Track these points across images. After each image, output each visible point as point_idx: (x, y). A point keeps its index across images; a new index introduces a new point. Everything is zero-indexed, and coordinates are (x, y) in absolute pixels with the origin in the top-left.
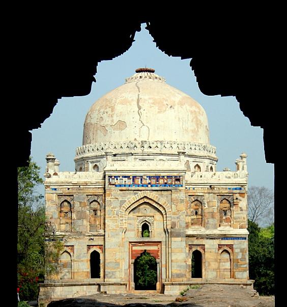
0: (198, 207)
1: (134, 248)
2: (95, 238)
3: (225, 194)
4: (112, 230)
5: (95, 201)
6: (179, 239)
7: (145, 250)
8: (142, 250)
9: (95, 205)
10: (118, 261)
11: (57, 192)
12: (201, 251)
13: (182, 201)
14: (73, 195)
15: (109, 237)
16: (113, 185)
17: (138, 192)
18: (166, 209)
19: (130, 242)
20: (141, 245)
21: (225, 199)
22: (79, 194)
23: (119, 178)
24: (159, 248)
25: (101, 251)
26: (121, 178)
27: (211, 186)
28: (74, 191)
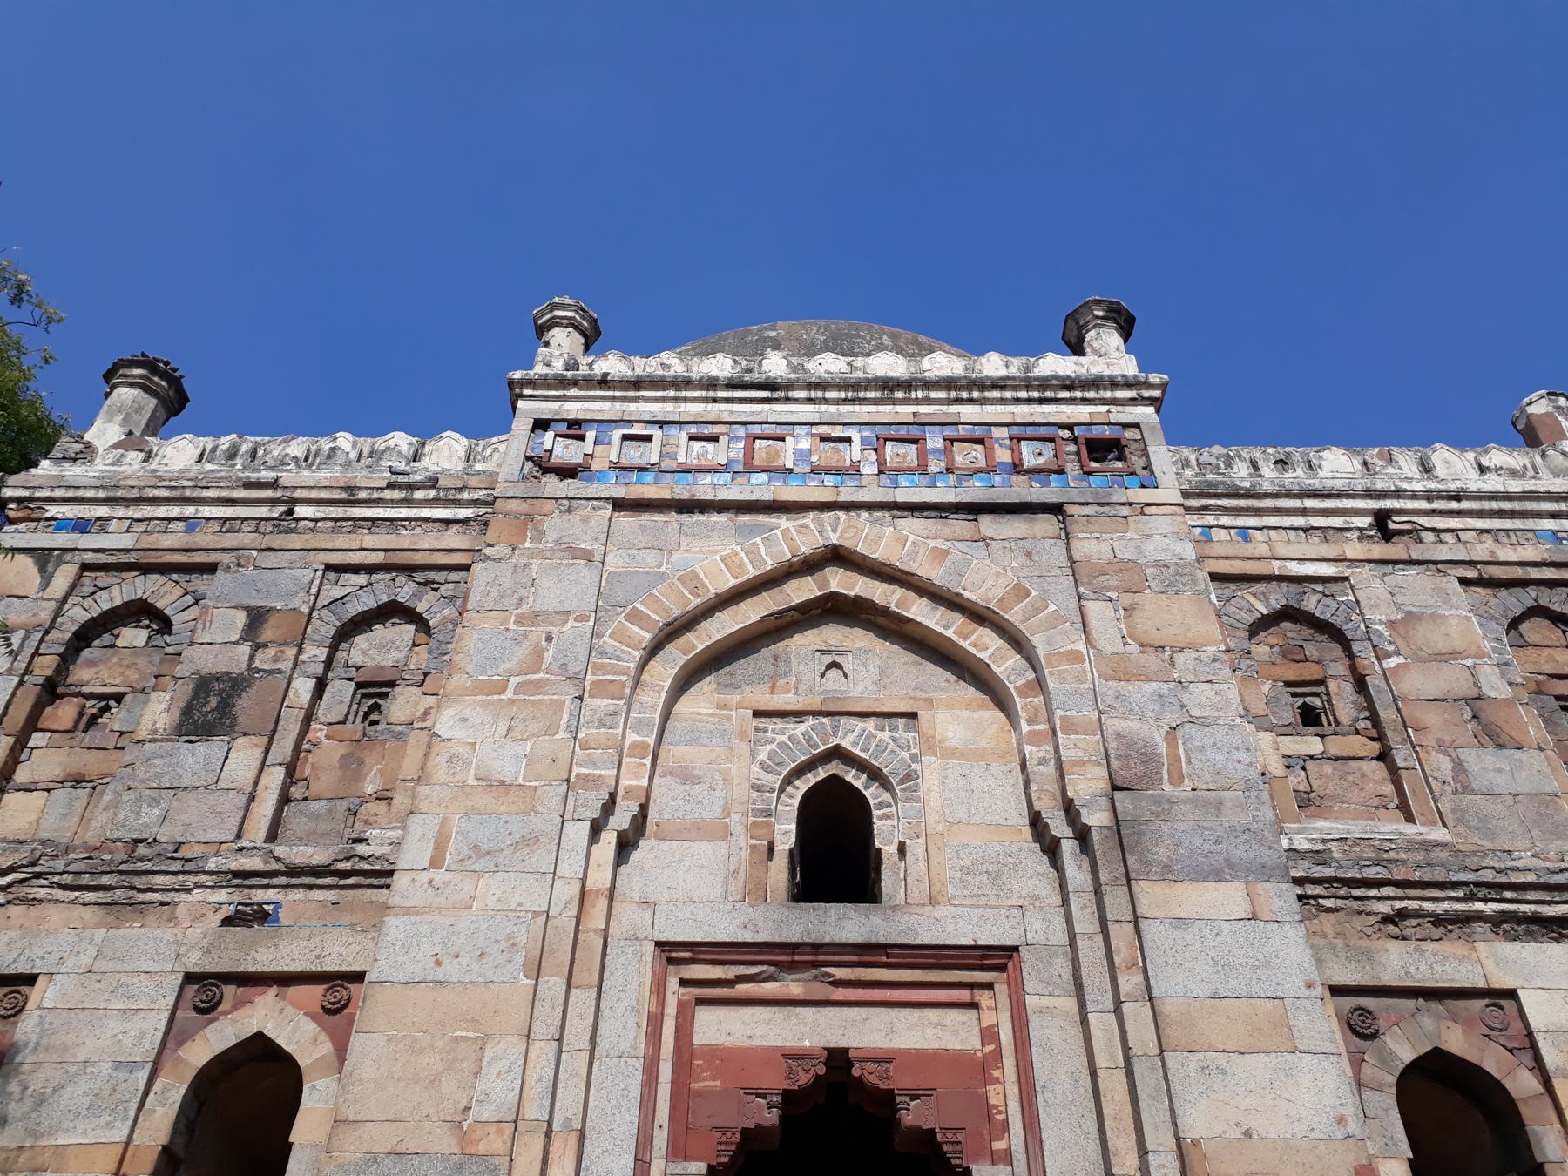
0: (1309, 672)
1: (718, 1028)
2: (291, 901)
3: (1534, 573)
4: (483, 801)
5: (391, 611)
6: (1229, 897)
7: (838, 1059)
8: (792, 1056)
9: (383, 647)
10: (495, 1143)
11: (85, 541)
12: (1490, 1066)
13: (1173, 580)
14: (211, 568)
15: (436, 862)
16: (567, 472)
17: (762, 519)
18: (1039, 642)
19: (671, 952)
20: (793, 986)
21: (1537, 611)
22: (272, 559)
23: (617, 434)
24: (989, 1035)
25: (326, 1047)
26: (638, 430)
27: (1381, 518)
28: (230, 540)
